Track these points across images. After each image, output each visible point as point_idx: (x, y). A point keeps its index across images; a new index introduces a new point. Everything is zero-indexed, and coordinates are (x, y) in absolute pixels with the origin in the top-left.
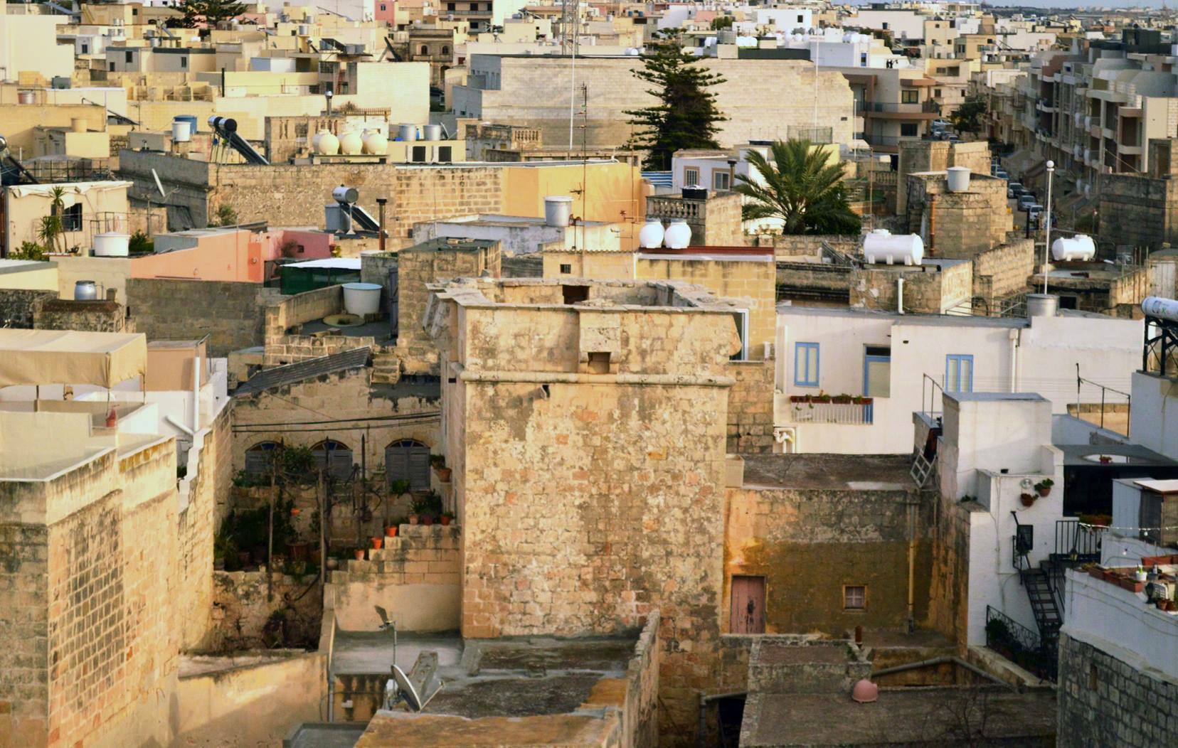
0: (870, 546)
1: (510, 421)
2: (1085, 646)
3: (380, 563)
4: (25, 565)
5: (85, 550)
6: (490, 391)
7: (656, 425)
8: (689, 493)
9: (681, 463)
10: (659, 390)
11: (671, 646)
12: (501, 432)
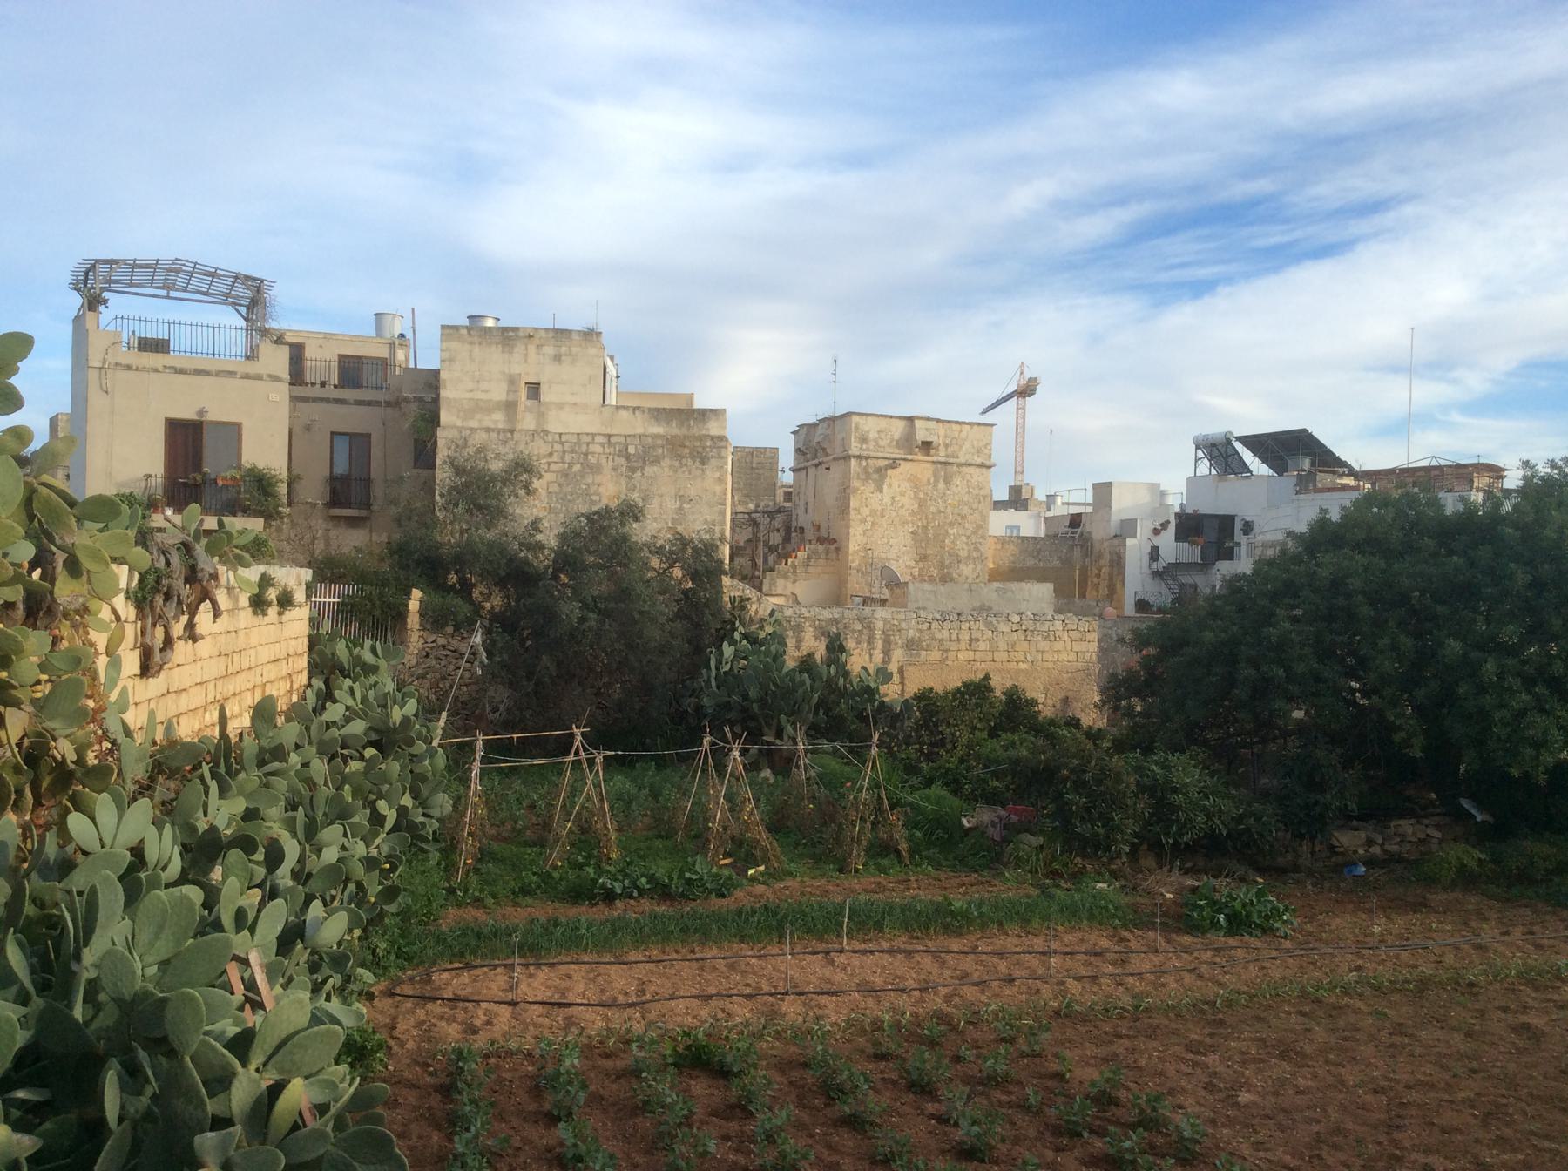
3: (795, 567)
4: (713, 462)
7: (953, 488)
8: (970, 527)
9: (966, 510)
12: (871, 486)
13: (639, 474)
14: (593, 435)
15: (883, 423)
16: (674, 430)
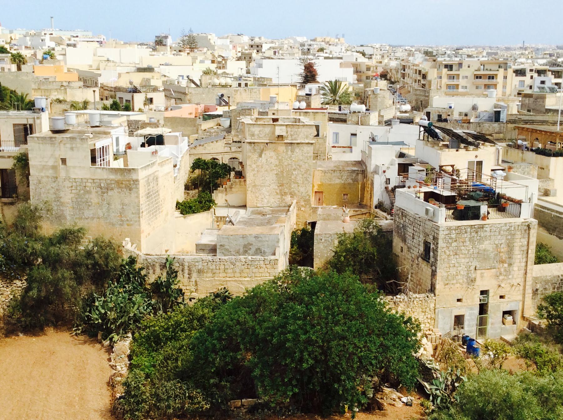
0: (349, 184)
2: (400, 209)
3: (226, 189)
4: (134, 189)
5: (149, 185)
6: (253, 145)
9: (301, 163)
11: (299, 209)
13: (106, 194)
14: (87, 180)
16: (118, 177)
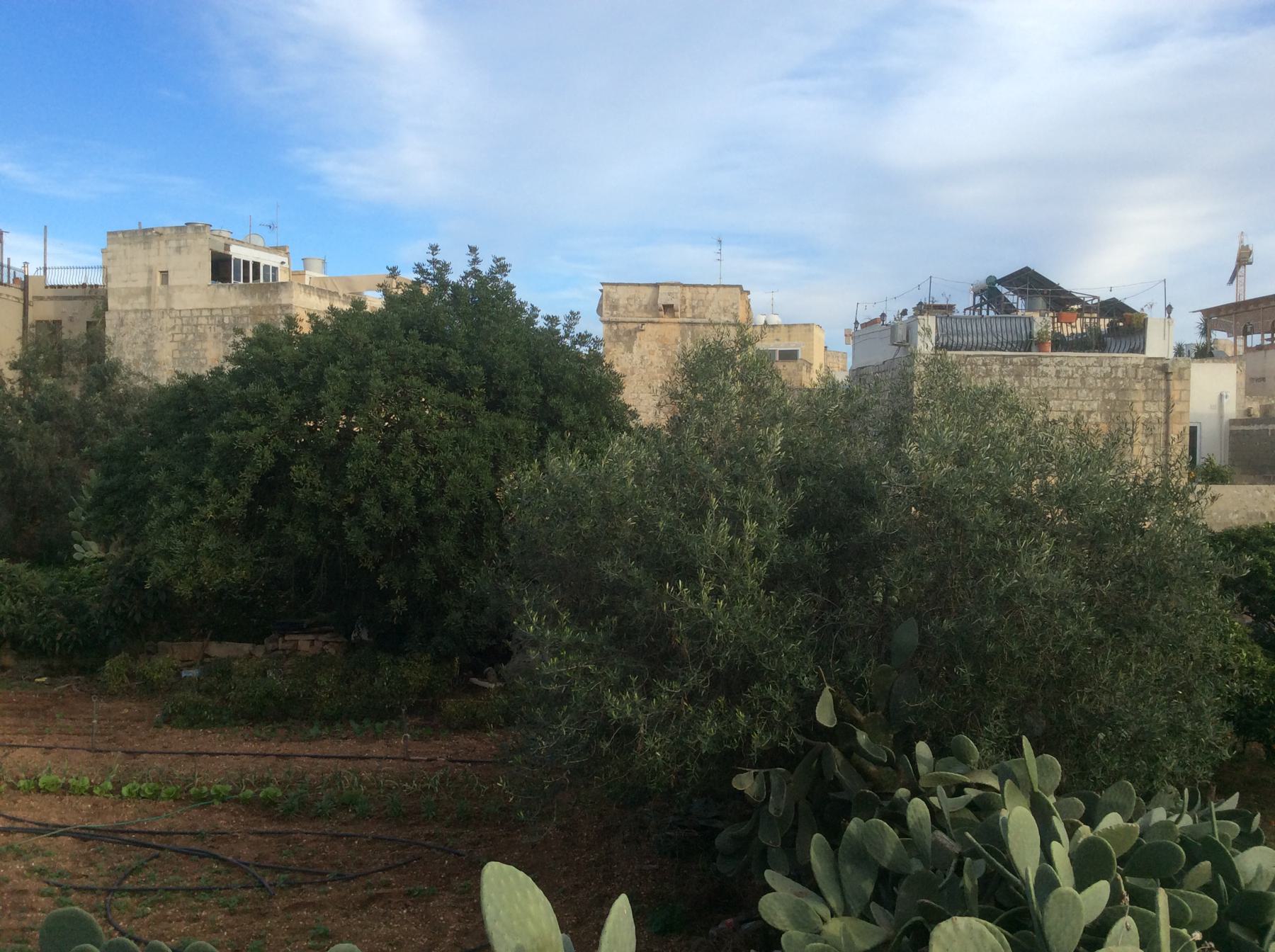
1: (625, 343)
6: (615, 327)
10: (701, 327)
14: (201, 310)
15: (633, 289)
